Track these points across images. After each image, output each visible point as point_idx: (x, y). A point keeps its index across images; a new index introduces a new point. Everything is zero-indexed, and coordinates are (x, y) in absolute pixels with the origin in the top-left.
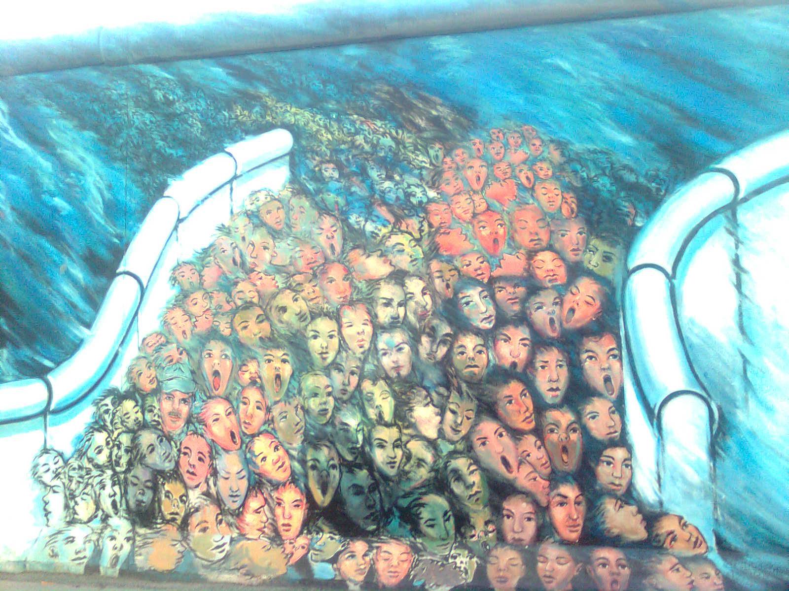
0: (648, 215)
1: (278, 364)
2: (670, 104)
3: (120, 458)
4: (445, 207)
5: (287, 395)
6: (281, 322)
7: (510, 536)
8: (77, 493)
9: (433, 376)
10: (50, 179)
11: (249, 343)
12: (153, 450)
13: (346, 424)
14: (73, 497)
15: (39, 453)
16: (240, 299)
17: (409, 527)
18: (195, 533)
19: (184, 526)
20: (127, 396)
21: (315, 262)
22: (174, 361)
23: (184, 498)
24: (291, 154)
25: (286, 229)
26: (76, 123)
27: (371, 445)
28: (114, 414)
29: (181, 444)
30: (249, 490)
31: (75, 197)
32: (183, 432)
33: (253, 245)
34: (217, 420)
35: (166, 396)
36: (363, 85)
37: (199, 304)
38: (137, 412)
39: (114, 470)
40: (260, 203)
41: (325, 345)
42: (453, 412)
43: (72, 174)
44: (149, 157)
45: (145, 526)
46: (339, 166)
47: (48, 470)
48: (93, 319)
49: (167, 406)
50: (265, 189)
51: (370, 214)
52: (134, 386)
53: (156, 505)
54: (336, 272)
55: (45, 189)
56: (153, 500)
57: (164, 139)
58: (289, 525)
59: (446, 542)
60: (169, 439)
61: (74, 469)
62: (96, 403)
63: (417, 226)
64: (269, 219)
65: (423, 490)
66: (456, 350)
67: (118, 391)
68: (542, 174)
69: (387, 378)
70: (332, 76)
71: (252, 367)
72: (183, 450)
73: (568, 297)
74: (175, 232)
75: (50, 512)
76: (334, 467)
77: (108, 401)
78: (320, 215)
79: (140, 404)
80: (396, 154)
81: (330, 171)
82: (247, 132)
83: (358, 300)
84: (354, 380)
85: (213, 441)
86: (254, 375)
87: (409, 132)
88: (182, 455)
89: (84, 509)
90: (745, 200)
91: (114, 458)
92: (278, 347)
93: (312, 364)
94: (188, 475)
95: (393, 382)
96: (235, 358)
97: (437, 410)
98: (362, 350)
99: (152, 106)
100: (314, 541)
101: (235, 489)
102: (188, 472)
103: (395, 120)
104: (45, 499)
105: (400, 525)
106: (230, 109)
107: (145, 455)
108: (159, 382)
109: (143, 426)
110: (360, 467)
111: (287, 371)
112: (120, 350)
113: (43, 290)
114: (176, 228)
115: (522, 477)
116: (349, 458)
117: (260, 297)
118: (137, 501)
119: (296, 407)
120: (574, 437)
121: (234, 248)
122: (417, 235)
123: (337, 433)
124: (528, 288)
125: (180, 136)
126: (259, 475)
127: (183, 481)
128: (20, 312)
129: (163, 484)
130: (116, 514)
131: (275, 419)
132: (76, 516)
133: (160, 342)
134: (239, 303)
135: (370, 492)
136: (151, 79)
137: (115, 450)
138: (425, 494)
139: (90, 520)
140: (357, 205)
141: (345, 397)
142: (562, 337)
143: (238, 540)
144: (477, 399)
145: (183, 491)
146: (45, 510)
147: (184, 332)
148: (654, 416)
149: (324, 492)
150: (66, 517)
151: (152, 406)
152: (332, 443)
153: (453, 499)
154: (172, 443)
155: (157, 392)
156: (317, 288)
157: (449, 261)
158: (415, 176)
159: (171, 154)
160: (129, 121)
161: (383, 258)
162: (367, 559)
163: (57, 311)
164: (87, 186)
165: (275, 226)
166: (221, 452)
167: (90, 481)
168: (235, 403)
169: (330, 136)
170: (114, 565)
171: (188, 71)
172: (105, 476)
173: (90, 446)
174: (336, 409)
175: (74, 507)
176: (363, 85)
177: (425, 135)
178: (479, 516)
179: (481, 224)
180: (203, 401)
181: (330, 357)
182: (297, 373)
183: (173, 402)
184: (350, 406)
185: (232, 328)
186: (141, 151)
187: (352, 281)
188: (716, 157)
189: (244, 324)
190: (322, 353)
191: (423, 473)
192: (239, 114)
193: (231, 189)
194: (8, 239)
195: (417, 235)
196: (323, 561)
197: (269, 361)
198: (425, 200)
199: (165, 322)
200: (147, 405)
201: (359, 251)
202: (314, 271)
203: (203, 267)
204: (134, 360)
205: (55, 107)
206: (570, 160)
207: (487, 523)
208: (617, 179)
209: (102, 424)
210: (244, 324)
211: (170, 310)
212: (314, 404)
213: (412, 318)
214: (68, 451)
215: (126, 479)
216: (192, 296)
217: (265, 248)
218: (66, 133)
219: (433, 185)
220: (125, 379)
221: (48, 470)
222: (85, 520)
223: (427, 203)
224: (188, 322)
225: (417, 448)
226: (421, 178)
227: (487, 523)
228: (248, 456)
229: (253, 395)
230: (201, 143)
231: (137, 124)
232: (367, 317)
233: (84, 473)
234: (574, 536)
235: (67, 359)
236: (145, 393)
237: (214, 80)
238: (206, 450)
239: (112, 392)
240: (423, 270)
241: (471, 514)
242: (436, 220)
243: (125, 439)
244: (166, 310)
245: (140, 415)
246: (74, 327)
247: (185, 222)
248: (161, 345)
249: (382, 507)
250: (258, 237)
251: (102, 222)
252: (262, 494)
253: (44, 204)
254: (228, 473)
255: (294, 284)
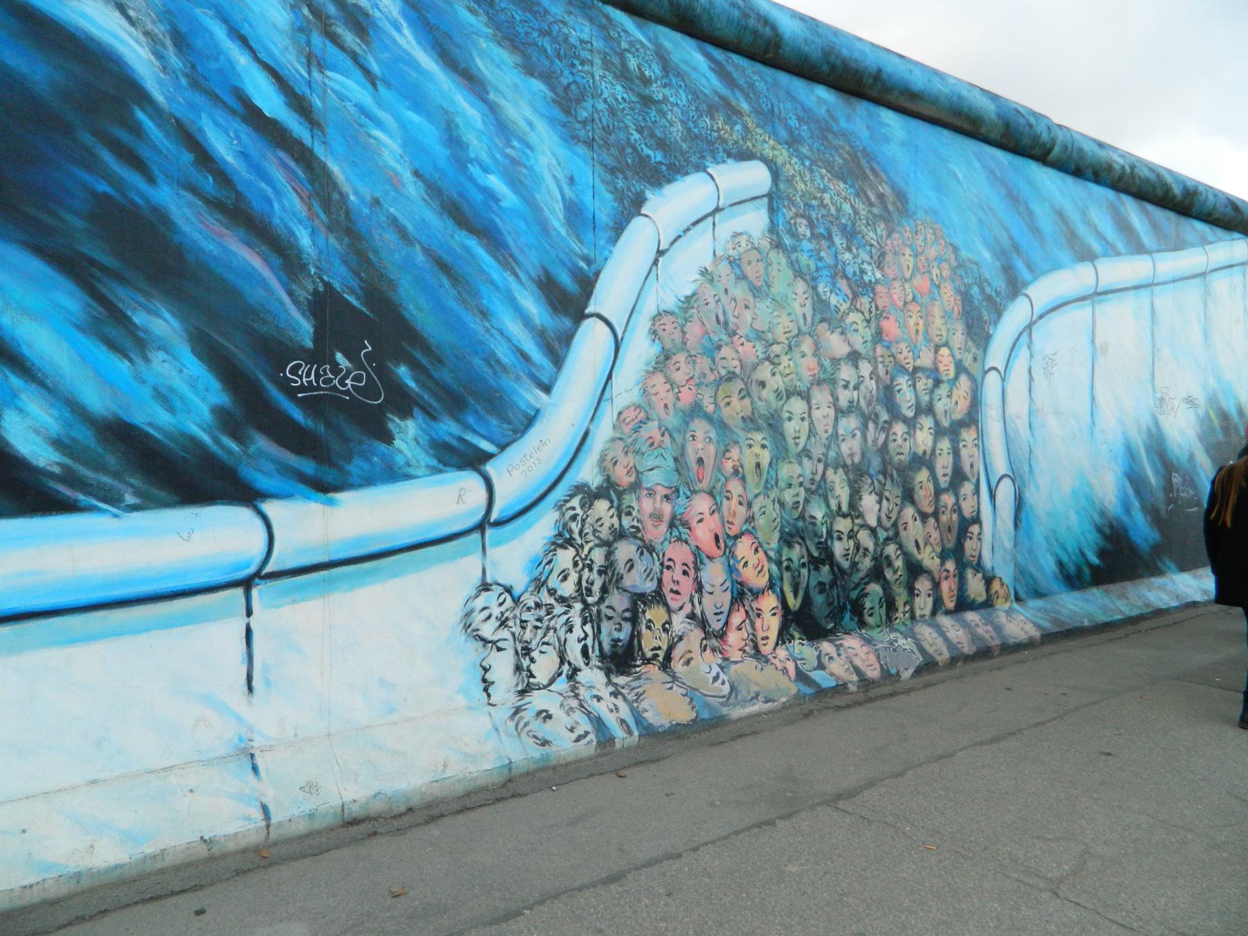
0: (996, 323)
1: (757, 449)
2: (1008, 231)
3: (592, 584)
4: (886, 290)
5: (766, 488)
6: (760, 399)
7: (918, 613)
8: (533, 645)
9: (876, 463)
10: (480, 140)
11: (731, 423)
12: (632, 567)
13: (813, 517)
14: (527, 651)
15: (474, 592)
16: (724, 368)
17: (856, 619)
18: (677, 666)
19: (666, 665)
20: (600, 493)
21: (789, 332)
22: (655, 445)
23: (667, 626)
24: (770, 196)
25: (764, 288)
26: (519, 59)
27: (832, 538)
28: (583, 521)
29: (664, 555)
30: (732, 604)
31: (520, 182)
32: (666, 539)
33: (735, 301)
34: (701, 521)
35: (646, 492)
36: (830, 137)
37: (682, 370)
38: (612, 517)
39: (584, 602)
40: (741, 250)
41: (797, 429)
42: (888, 500)
43: (515, 143)
44: (622, 150)
45: (622, 673)
46: (811, 225)
47: (489, 617)
48: (554, 380)
49: (648, 505)
50: (746, 233)
51: (834, 285)
52: (608, 479)
53: (636, 642)
54: (807, 346)
55: (472, 156)
56: (632, 637)
57: (640, 130)
58: (767, 638)
59: (880, 629)
60: (651, 549)
61: (529, 609)
62: (559, 507)
63: (868, 306)
64: (749, 271)
65: (867, 580)
66: (891, 438)
67: (589, 487)
68: (944, 273)
69: (845, 466)
70: (806, 116)
71: (735, 453)
72: (666, 563)
73: (955, 391)
74: (654, 268)
75: (493, 683)
76: (803, 565)
77: (575, 502)
78: (795, 277)
79: (615, 504)
80: (854, 224)
81: (804, 229)
82: (729, 155)
83: (824, 380)
84: (821, 467)
85: (697, 547)
86: (736, 463)
87: (863, 203)
88: (665, 570)
89: (544, 665)
90: (1035, 322)
91: (584, 584)
92: (758, 429)
93: (787, 450)
94: (672, 595)
95: (849, 471)
96: (718, 442)
97: (877, 498)
98: (826, 435)
99: (624, 75)
100: (791, 650)
101: (718, 606)
102: (672, 591)
103: (852, 186)
104: (484, 664)
105: (851, 619)
106: (712, 118)
107: (622, 577)
108: (638, 473)
109: (620, 535)
110: (823, 563)
111: (765, 457)
112: (591, 427)
113: (473, 323)
114: (656, 262)
115: (928, 558)
116: (816, 554)
117: (742, 366)
118: (613, 640)
119: (774, 501)
120: (955, 517)
121: (717, 302)
122: (868, 317)
123: (806, 528)
124: (934, 380)
125: (658, 133)
126: (741, 584)
127: (666, 605)
128: (440, 361)
129: (644, 612)
130: (587, 664)
131: (756, 517)
132: (532, 680)
133: (639, 419)
134: (723, 372)
135: (831, 587)
136: (622, 34)
137: (586, 573)
138: (867, 583)
139: (552, 681)
140: (825, 273)
141: (813, 487)
142: (951, 426)
143: (728, 667)
144: (903, 486)
145: (666, 617)
146: (484, 680)
147: (666, 406)
148: (992, 496)
149: (796, 596)
150: (517, 685)
151: (630, 507)
152: (803, 539)
153: (886, 586)
154: (654, 555)
155: (635, 486)
156: (791, 363)
157: (888, 348)
158: (866, 251)
159: (648, 156)
160: (595, 87)
161: (843, 336)
162: (843, 657)
163: (498, 361)
164: (537, 168)
165: (755, 281)
166: (706, 561)
167: (552, 623)
168: (718, 499)
169: (803, 186)
170: (630, 732)
171: (668, 45)
172: (572, 611)
173: (551, 571)
174: (807, 501)
175: (528, 667)
176: (830, 137)
177: (875, 211)
178: (901, 596)
179: (910, 313)
180: (687, 498)
181: (802, 442)
182: (774, 461)
183: (655, 499)
184: (816, 498)
185: (717, 405)
186: (613, 137)
187: (819, 358)
188: (1025, 284)
189: (727, 400)
190: (795, 438)
191: (867, 564)
192: (720, 126)
193: (714, 224)
194: (410, 228)
195: (868, 317)
196: (815, 669)
197: (750, 446)
198: (873, 281)
199: (645, 391)
200: (624, 506)
201: (825, 325)
202: (790, 343)
203: (686, 320)
204: (607, 442)
205: (484, 19)
206: (959, 266)
207: (905, 604)
208: (982, 290)
209: (568, 536)
210: (727, 400)
211: (650, 374)
212: (788, 496)
213: (863, 403)
214: (519, 581)
215: (599, 612)
216: (675, 358)
217: (747, 307)
218: (502, 70)
219: (880, 266)
220: (596, 470)
221: (489, 617)
222: (545, 683)
223: (875, 283)
224: (670, 393)
225: (864, 538)
226: (871, 257)
227: (905, 604)
228: (732, 562)
229: (735, 487)
230: (682, 154)
231: (605, 95)
232: (830, 399)
233: (542, 612)
234: (950, 605)
235: (519, 438)
236: (621, 489)
237: (695, 69)
238: (690, 560)
239: (580, 489)
240: (871, 353)
241: (897, 598)
242: (880, 303)
243: (598, 556)
244: (644, 373)
245: (615, 520)
246: (526, 389)
247: (667, 255)
248: (641, 422)
249: (839, 603)
250: (740, 291)
251: (563, 232)
252: (744, 606)
253: (471, 179)
254: (713, 586)
255: (772, 356)
